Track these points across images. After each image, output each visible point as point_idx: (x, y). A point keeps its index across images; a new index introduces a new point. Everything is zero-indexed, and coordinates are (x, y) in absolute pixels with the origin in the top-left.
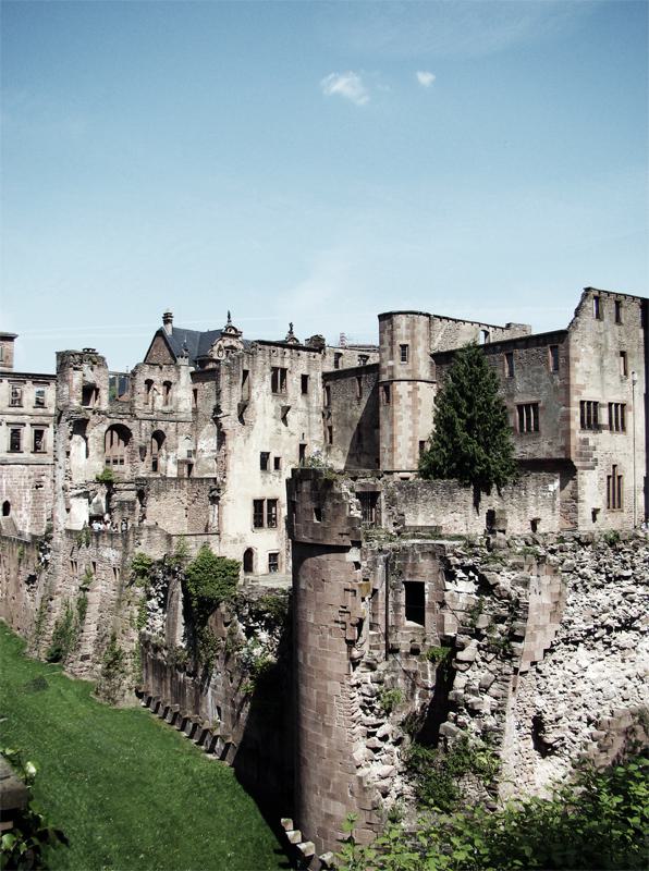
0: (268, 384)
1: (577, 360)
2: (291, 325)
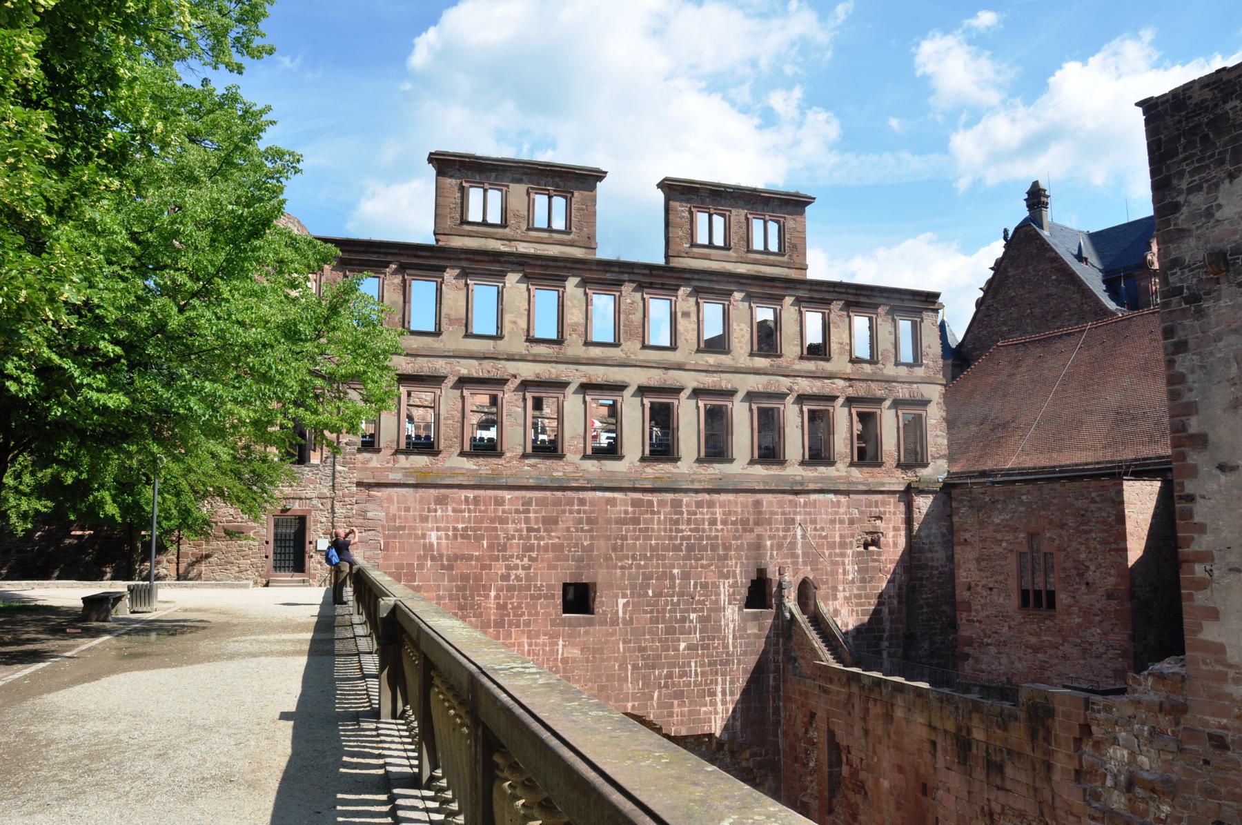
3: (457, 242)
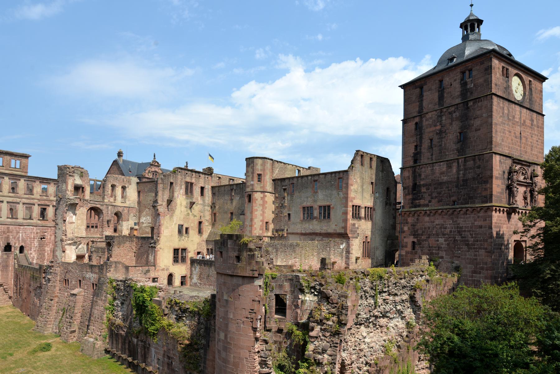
0: (183, 191)
1: (352, 185)
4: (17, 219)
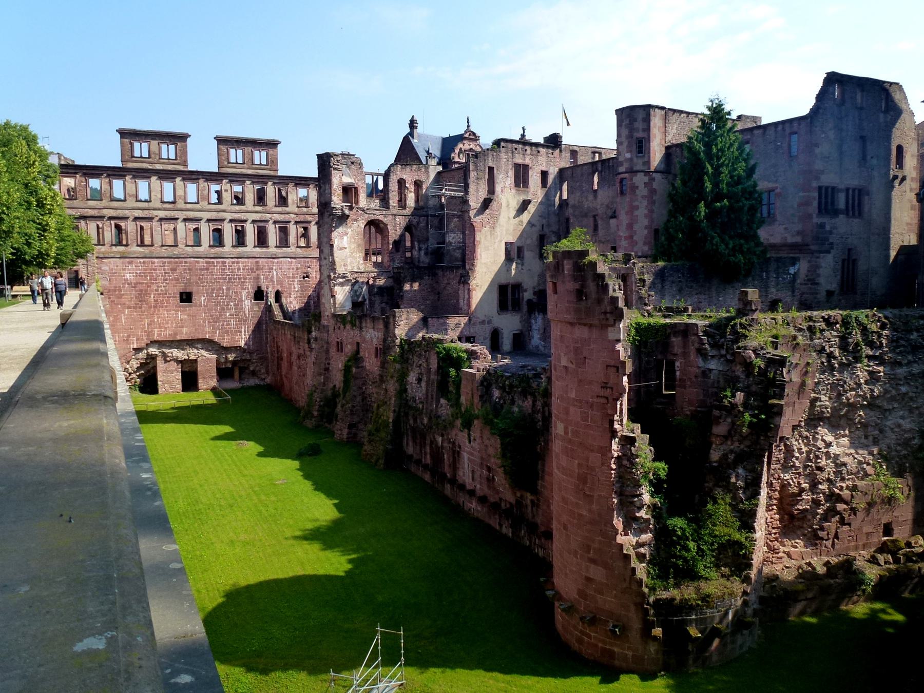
2: (524, 129)
3: (130, 165)
4: (268, 247)
